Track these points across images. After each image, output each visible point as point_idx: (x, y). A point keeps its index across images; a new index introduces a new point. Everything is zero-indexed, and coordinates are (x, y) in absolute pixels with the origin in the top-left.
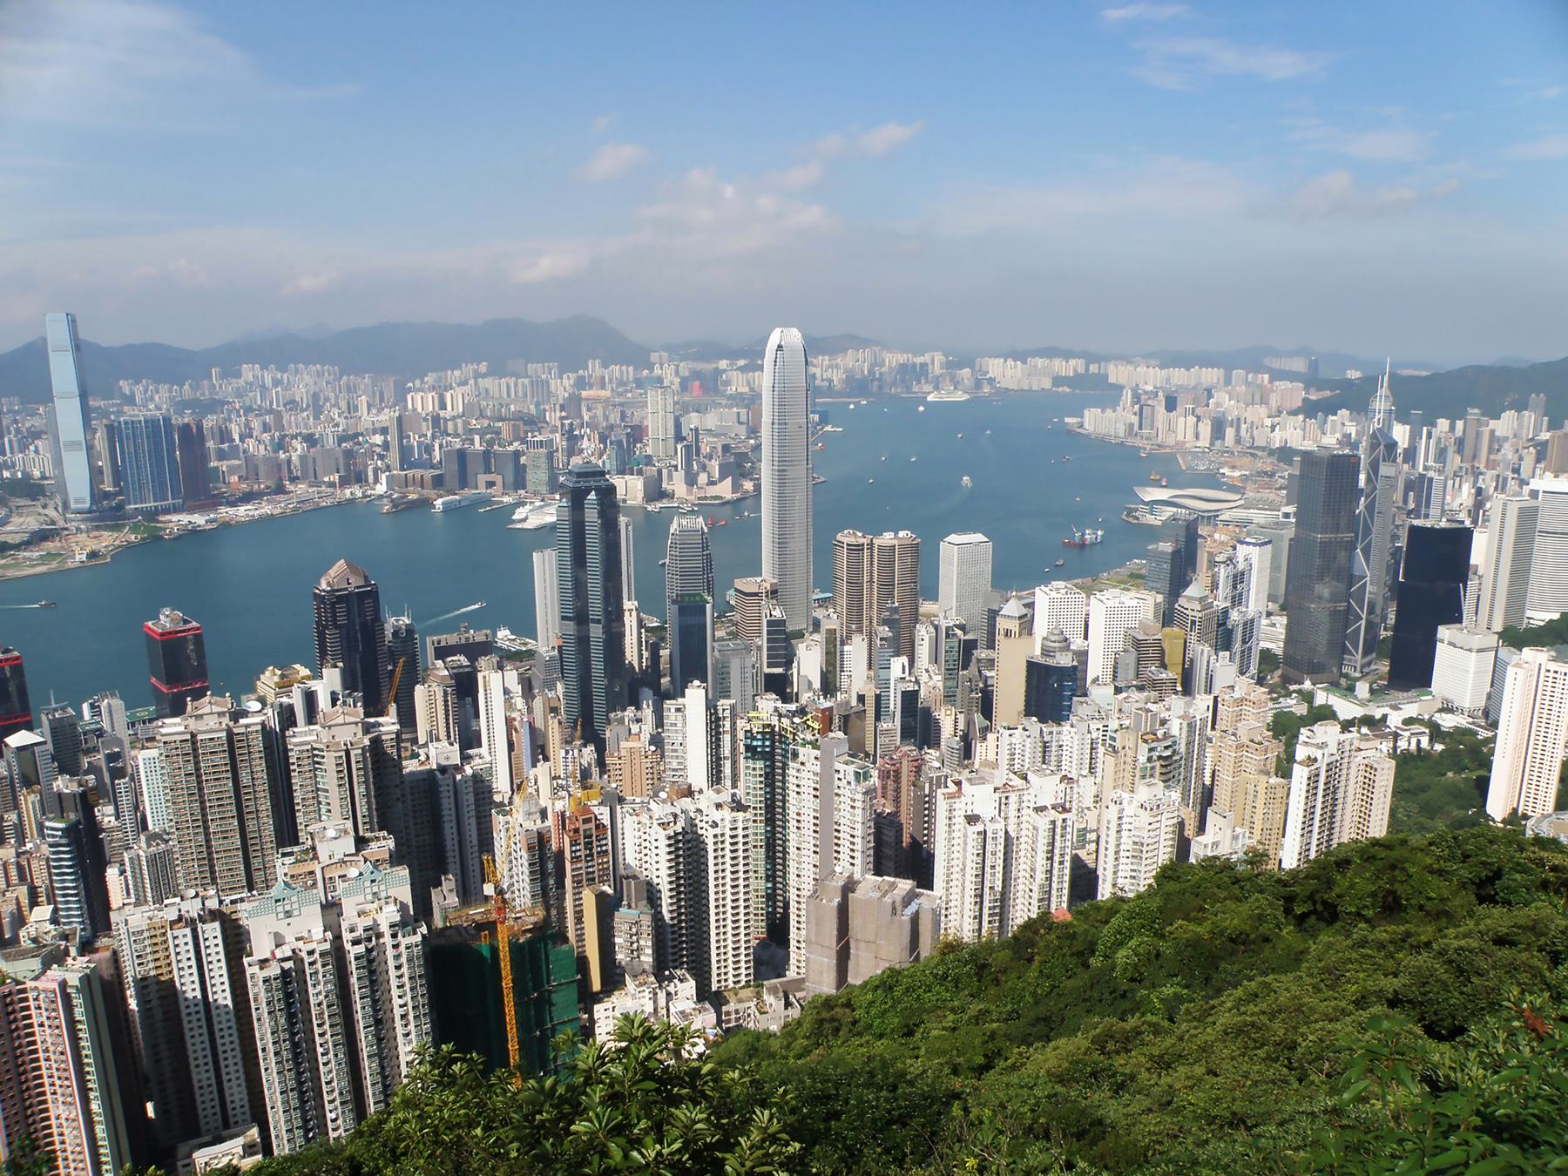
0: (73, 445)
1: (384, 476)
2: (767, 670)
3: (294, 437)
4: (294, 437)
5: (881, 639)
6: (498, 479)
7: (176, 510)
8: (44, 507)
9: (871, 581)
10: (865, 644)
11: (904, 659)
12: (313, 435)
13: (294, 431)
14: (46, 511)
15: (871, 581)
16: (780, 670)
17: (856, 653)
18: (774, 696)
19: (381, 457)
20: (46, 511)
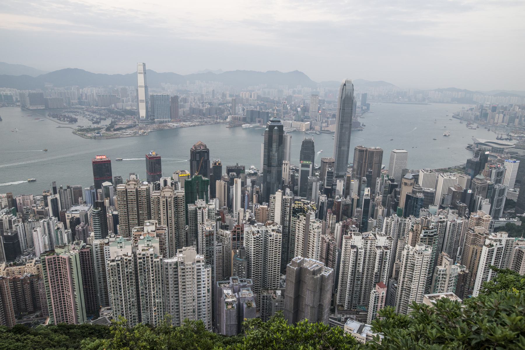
0: (142, 101)
1: (229, 117)
2: (326, 187)
3: (206, 103)
4: (206, 103)
5: (363, 181)
6: (262, 120)
7: (169, 122)
8: (134, 118)
9: (365, 162)
10: (358, 182)
11: (369, 188)
12: (211, 102)
13: (206, 101)
14: (134, 119)
15: (365, 162)
16: (330, 187)
17: (355, 183)
18: (326, 196)
19: (229, 111)
20: (134, 119)
